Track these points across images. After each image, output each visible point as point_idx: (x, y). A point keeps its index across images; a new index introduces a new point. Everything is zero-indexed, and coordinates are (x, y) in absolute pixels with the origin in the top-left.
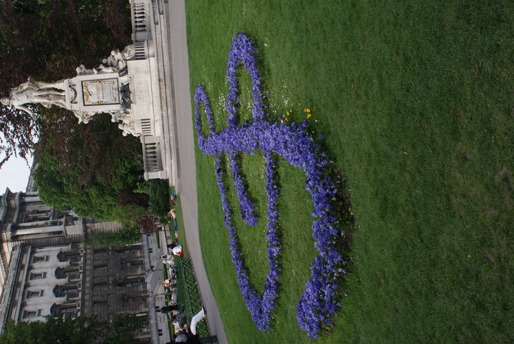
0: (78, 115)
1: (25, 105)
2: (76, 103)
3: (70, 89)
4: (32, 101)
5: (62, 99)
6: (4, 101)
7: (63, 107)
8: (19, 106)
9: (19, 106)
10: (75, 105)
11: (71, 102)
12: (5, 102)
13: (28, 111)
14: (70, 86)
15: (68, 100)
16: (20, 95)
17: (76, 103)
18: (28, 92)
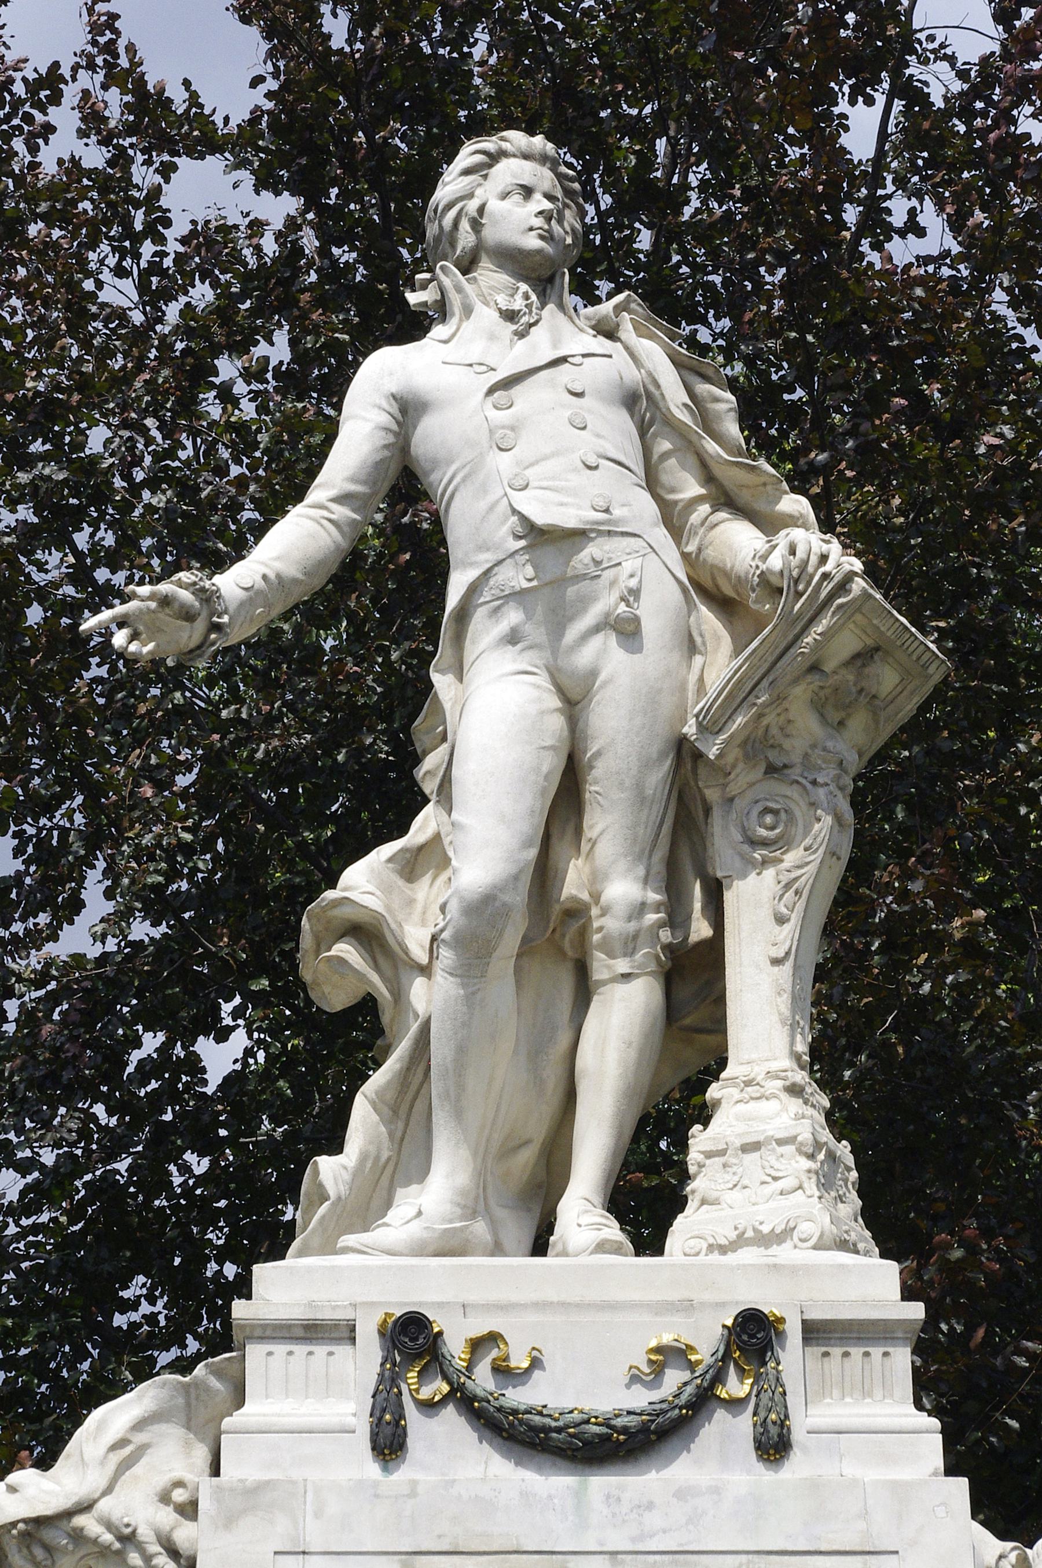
0: (128, 1453)
1: (400, 570)
2: (389, 1443)
3: (707, 1340)
4: (485, 632)
5: (474, 1205)
6: (510, 171)
7: (310, 1220)
8: (408, 410)
9: (408, 410)
10: (352, 1410)
11: (411, 1338)
12: (503, 187)
13: (296, 542)
14: (753, 1336)
15: (470, 1295)
16: (616, 433)
17: (389, 1443)
18: (646, 570)
